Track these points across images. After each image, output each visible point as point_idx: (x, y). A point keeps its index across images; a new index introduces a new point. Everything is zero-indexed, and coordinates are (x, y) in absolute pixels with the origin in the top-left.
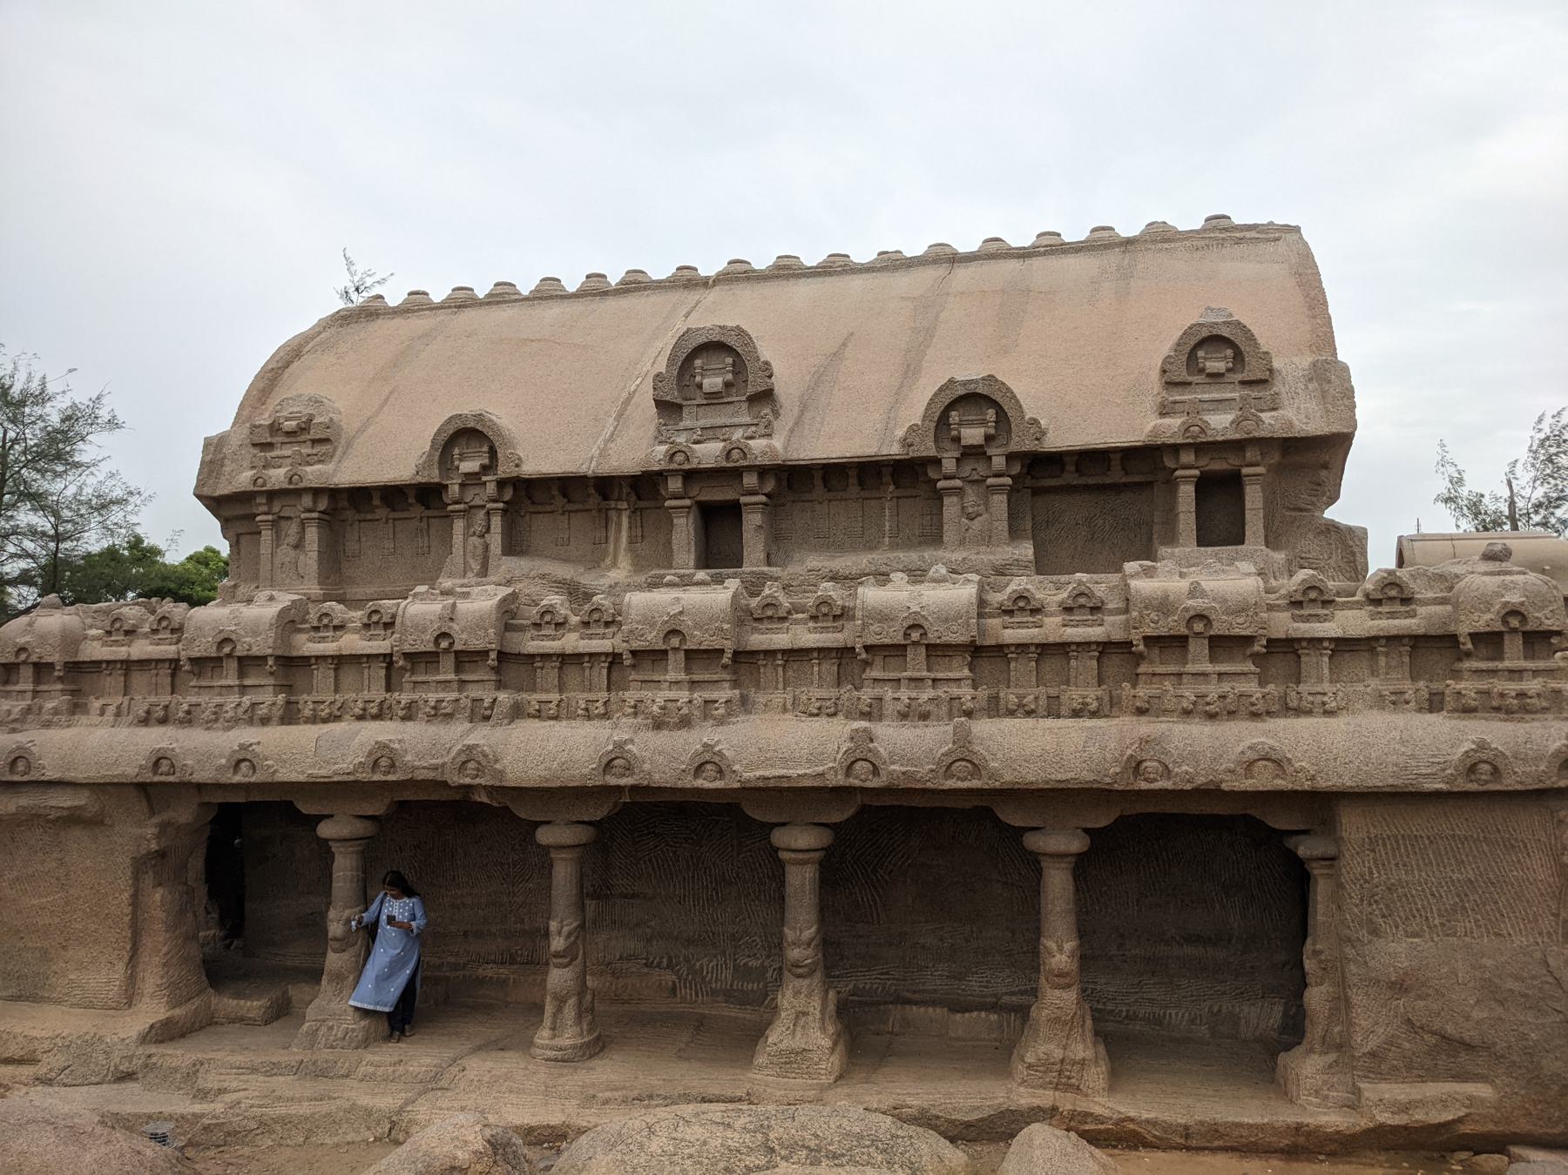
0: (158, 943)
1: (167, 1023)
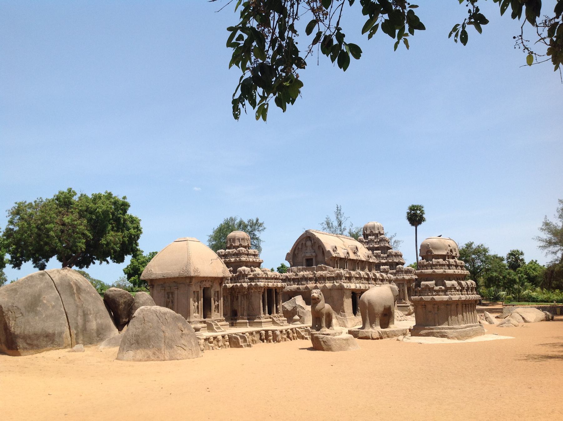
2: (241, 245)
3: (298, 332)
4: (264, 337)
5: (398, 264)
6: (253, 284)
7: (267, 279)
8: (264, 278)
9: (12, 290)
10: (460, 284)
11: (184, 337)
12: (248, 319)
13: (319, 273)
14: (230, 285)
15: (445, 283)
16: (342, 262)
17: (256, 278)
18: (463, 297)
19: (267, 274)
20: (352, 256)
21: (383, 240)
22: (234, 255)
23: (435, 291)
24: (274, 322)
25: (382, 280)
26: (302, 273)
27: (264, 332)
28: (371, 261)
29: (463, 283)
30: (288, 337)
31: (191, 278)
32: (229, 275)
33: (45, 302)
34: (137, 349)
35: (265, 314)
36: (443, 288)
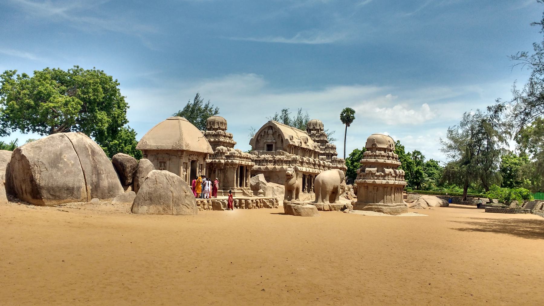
2: (219, 127)
3: (264, 202)
4: (238, 204)
5: (333, 155)
6: (230, 161)
7: (240, 157)
8: (238, 157)
9: (37, 147)
10: (395, 172)
11: (187, 197)
12: (223, 189)
13: (278, 157)
14: (209, 161)
15: (384, 170)
16: (296, 149)
17: (232, 156)
18: (397, 182)
19: (240, 153)
20: (304, 146)
21: (322, 135)
22: (213, 135)
23: (376, 176)
24: (244, 194)
25: (324, 167)
26: (263, 156)
27: (238, 200)
28: (316, 150)
29: (397, 171)
30: (257, 205)
31: (182, 151)
32: (211, 151)
33: (65, 160)
34: (151, 204)
35: (237, 186)
36: (383, 174)
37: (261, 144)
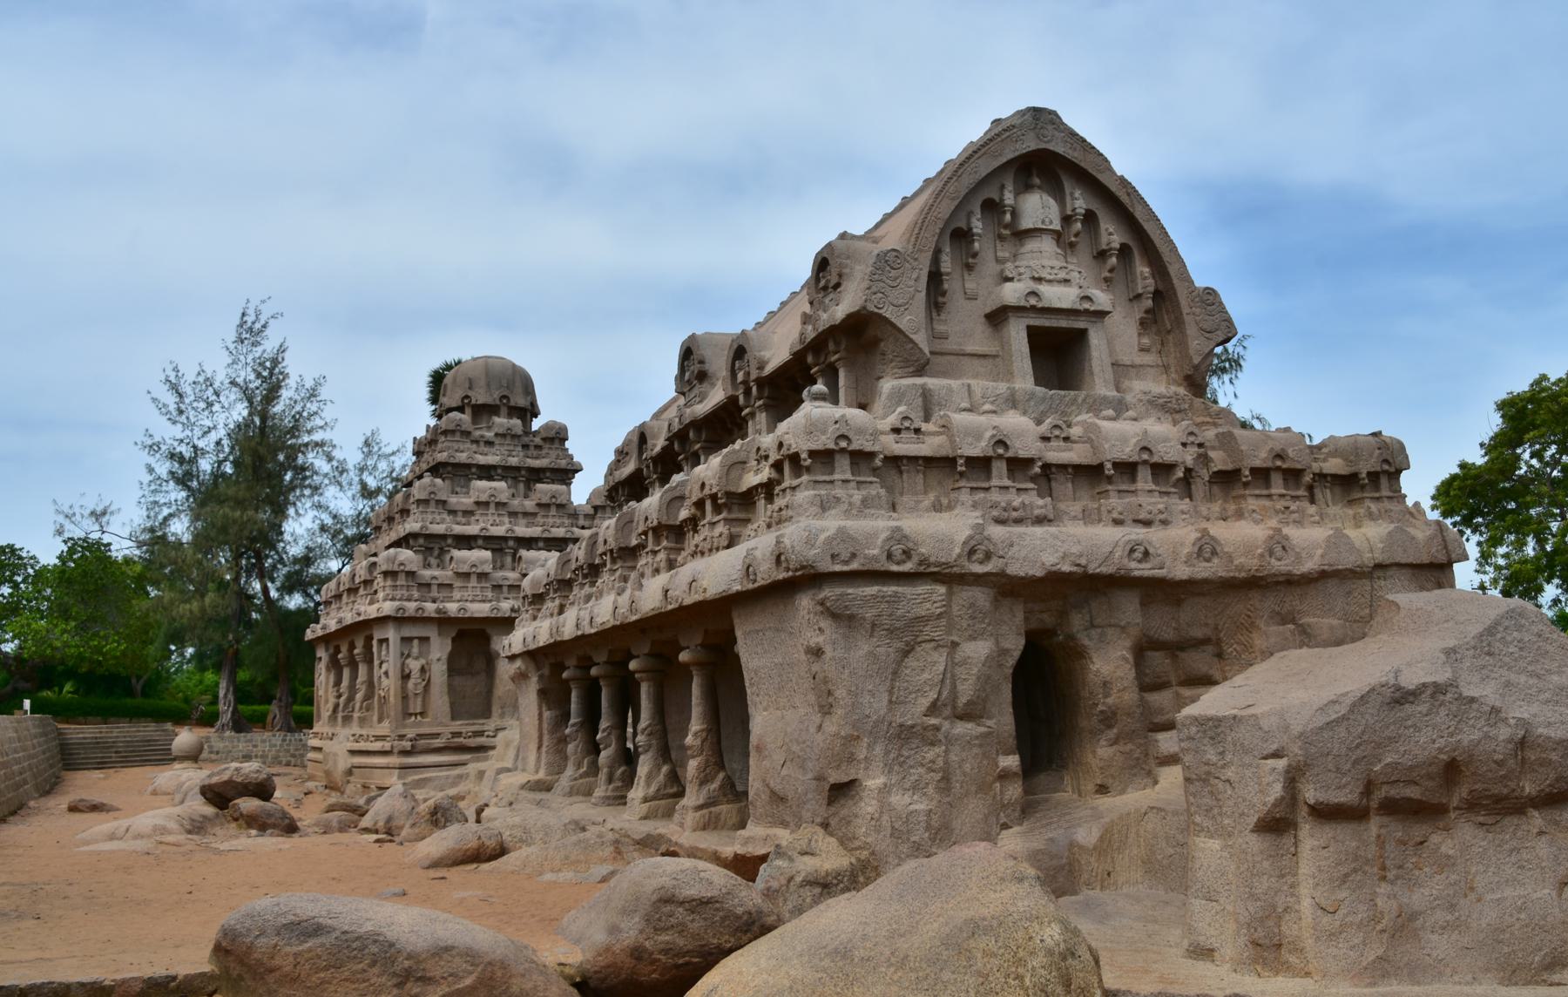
0: (546, 738)
1: (538, 782)
37: (964, 324)
